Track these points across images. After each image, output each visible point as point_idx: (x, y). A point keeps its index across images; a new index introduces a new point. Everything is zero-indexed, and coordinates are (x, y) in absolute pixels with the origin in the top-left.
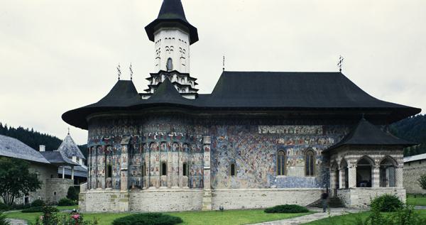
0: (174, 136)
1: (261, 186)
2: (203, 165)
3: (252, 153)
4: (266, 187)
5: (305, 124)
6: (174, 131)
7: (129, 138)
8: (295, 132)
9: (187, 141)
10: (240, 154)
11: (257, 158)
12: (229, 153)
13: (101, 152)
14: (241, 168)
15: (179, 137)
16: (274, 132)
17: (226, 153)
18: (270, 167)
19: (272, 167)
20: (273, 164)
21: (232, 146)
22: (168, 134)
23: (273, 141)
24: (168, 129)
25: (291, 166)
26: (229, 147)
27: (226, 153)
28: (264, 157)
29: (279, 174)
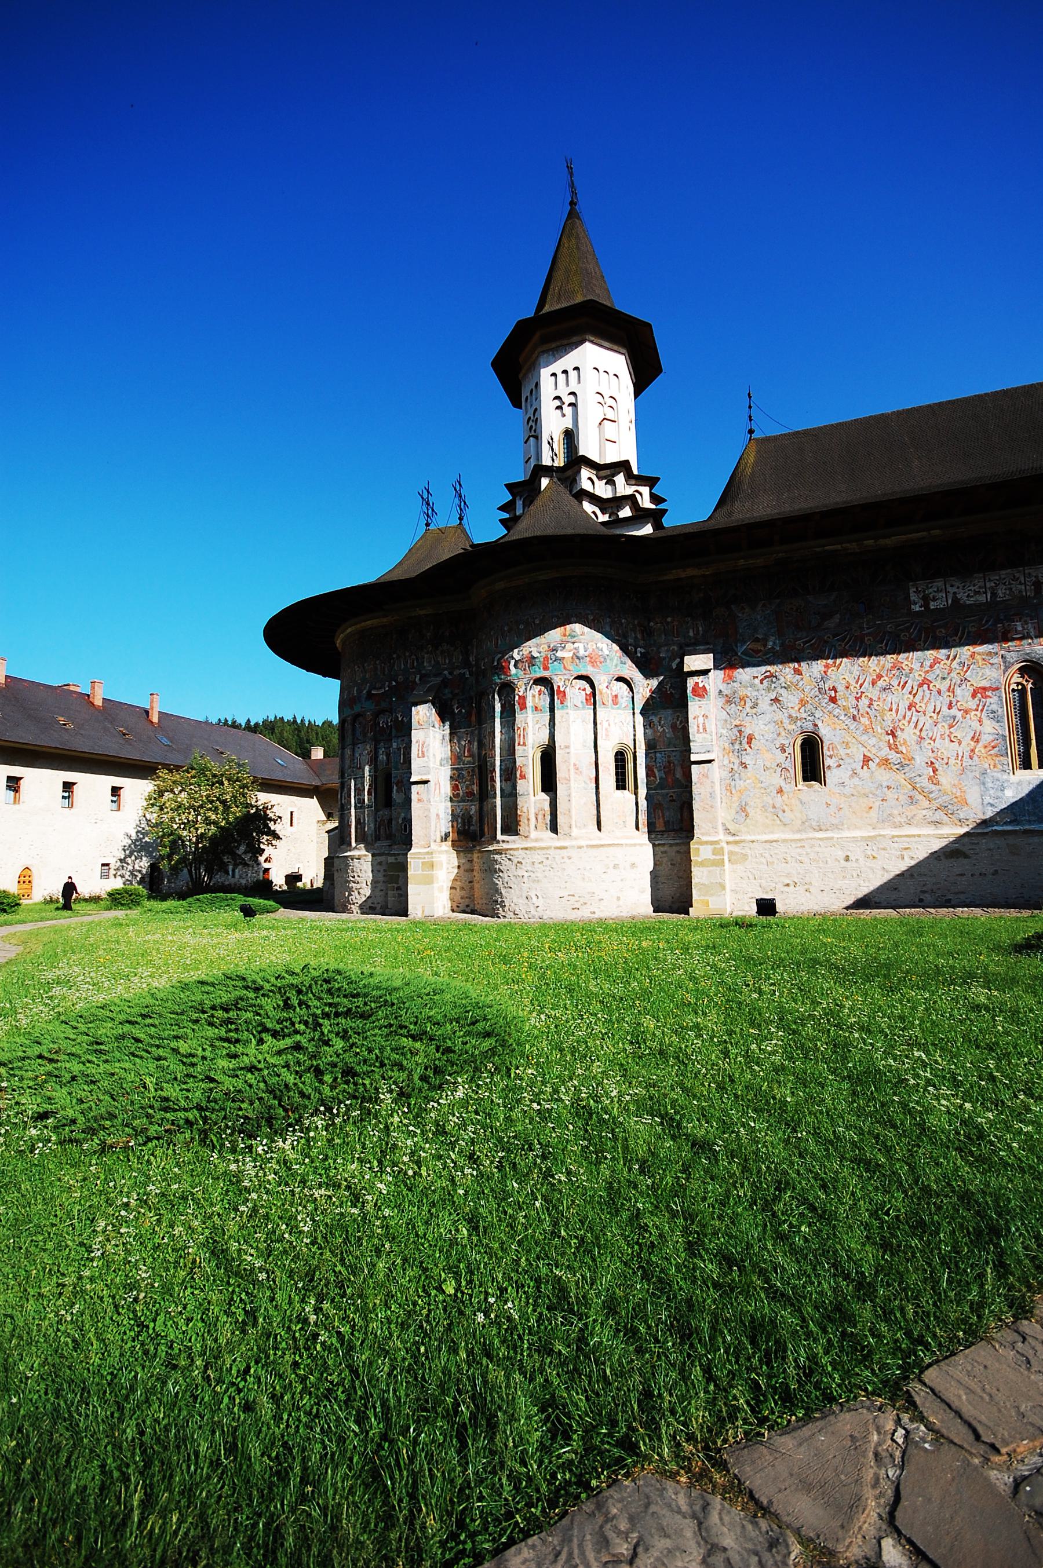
1: (940, 815)
2: (689, 751)
7: (439, 679)
10: (833, 700)
12: (791, 699)
13: (365, 735)
16: (982, 598)
17: (776, 700)
18: (975, 738)
19: (986, 739)
20: (989, 728)
27: (776, 700)
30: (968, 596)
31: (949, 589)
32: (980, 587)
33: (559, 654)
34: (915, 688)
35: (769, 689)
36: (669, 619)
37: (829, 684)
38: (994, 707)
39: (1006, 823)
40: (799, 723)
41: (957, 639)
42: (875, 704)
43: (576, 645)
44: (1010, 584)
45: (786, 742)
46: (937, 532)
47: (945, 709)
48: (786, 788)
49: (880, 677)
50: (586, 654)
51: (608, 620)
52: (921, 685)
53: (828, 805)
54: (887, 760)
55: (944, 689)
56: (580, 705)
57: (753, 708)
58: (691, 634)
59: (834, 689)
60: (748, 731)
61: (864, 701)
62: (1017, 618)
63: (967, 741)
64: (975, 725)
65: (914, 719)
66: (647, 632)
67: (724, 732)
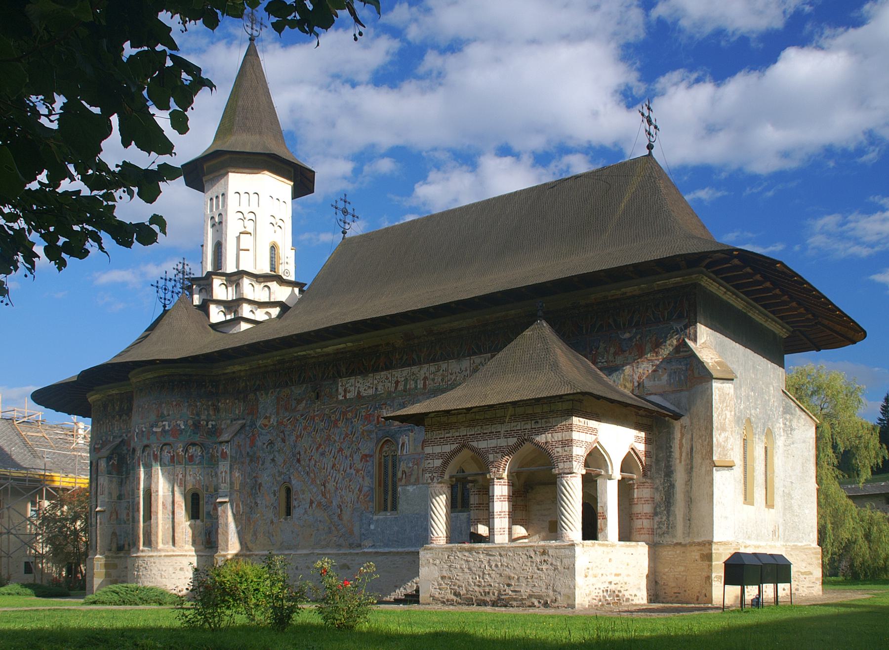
0: (164, 431)
3: (323, 454)
4: (351, 546)
5: (445, 358)
6: (161, 417)
8: (420, 385)
9: (197, 439)
11: (334, 466)
12: (280, 459)
14: (301, 496)
15: (176, 432)
16: (371, 392)
17: (273, 460)
18: (360, 490)
19: (365, 489)
20: (367, 482)
21: (284, 441)
22: (152, 427)
23: (368, 418)
24: (153, 417)
25: (408, 483)
26: (278, 444)
28: (348, 462)
29: (385, 509)
30: (365, 390)
31: (357, 384)
32: (371, 384)
33: (154, 429)
34: (336, 453)
35: (270, 453)
36: (228, 401)
37: (297, 450)
38: (370, 468)
39: (370, 547)
40: (283, 476)
41: (356, 420)
42: (317, 464)
43: (164, 423)
44: (385, 382)
45: (276, 489)
46: (349, 344)
47: (349, 468)
48: (275, 521)
49: (320, 445)
50: (169, 428)
51: (186, 404)
52: (338, 452)
53: (293, 532)
54: (321, 503)
55: (348, 455)
56: (167, 463)
57: (262, 465)
58: (237, 412)
59: (299, 453)
60: (259, 481)
61: (313, 462)
62: (384, 406)
63: (356, 491)
64: (360, 480)
65: (334, 475)
66: (217, 410)
67: (249, 481)
